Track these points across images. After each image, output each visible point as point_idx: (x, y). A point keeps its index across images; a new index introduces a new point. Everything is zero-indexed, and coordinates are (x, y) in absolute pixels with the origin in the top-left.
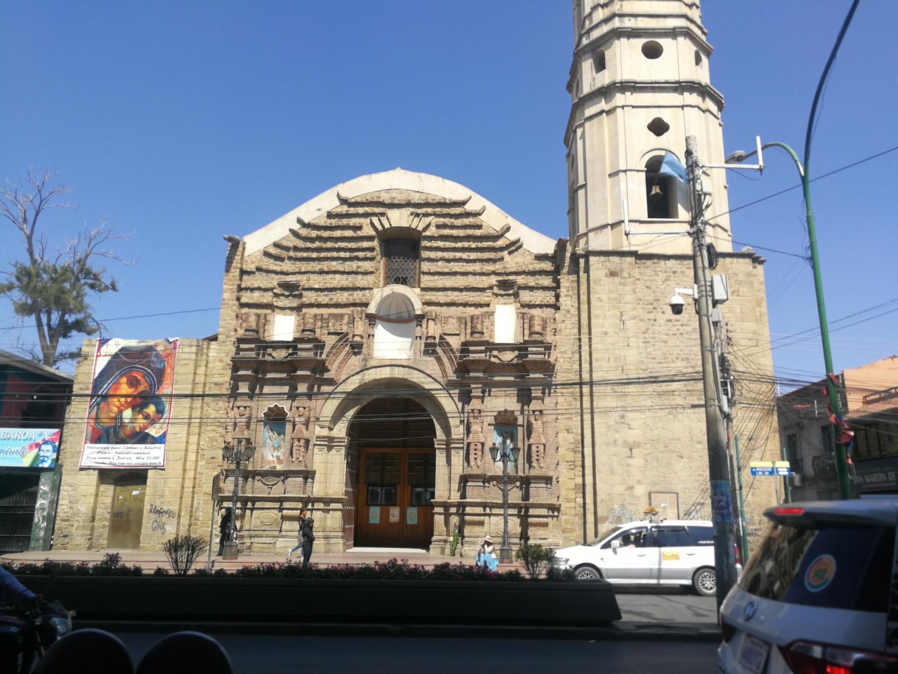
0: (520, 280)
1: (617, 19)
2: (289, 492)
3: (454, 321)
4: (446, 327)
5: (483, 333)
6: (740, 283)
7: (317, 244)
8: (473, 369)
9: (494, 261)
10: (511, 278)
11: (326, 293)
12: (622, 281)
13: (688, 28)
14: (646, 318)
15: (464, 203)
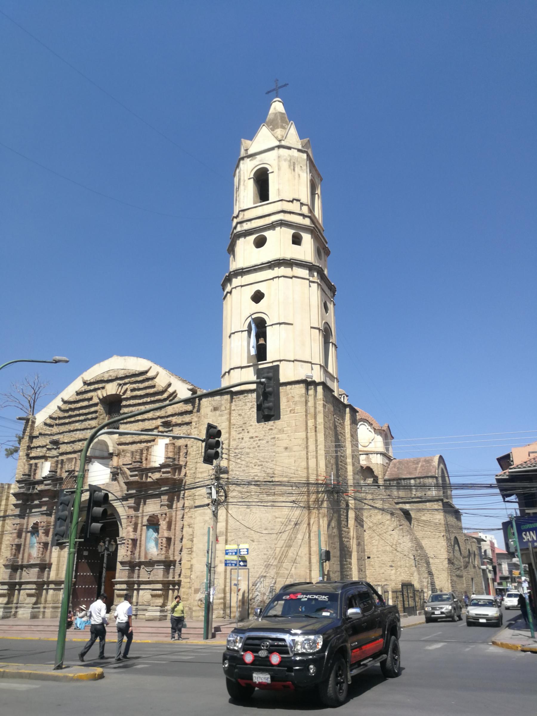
0: (174, 420)
1: (239, 225)
2: (30, 578)
3: (129, 455)
4: (125, 460)
5: (141, 462)
6: (296, 404)
7: (71, 413)
8: (142, 487)
9: (160, 408)
10: (169, 419)
11: (71, 444)
12: (221, 413)
13: (281, 220)
14: (237, 438)
15: (146, 372)
